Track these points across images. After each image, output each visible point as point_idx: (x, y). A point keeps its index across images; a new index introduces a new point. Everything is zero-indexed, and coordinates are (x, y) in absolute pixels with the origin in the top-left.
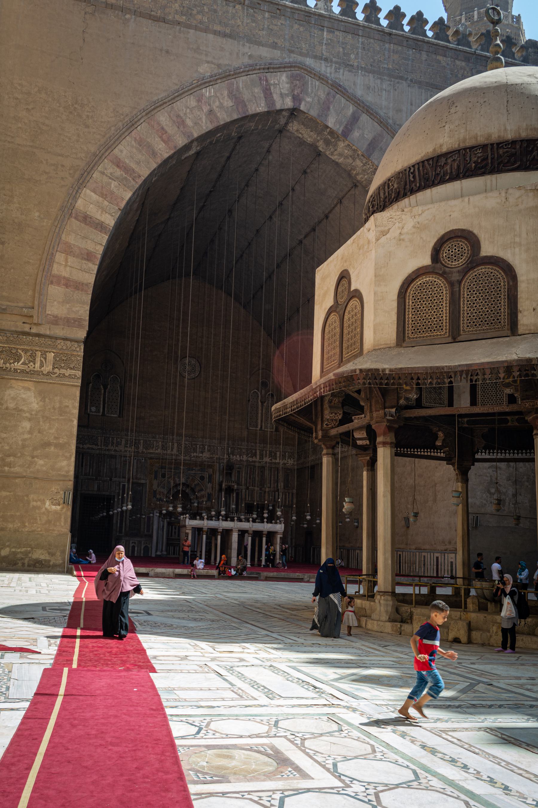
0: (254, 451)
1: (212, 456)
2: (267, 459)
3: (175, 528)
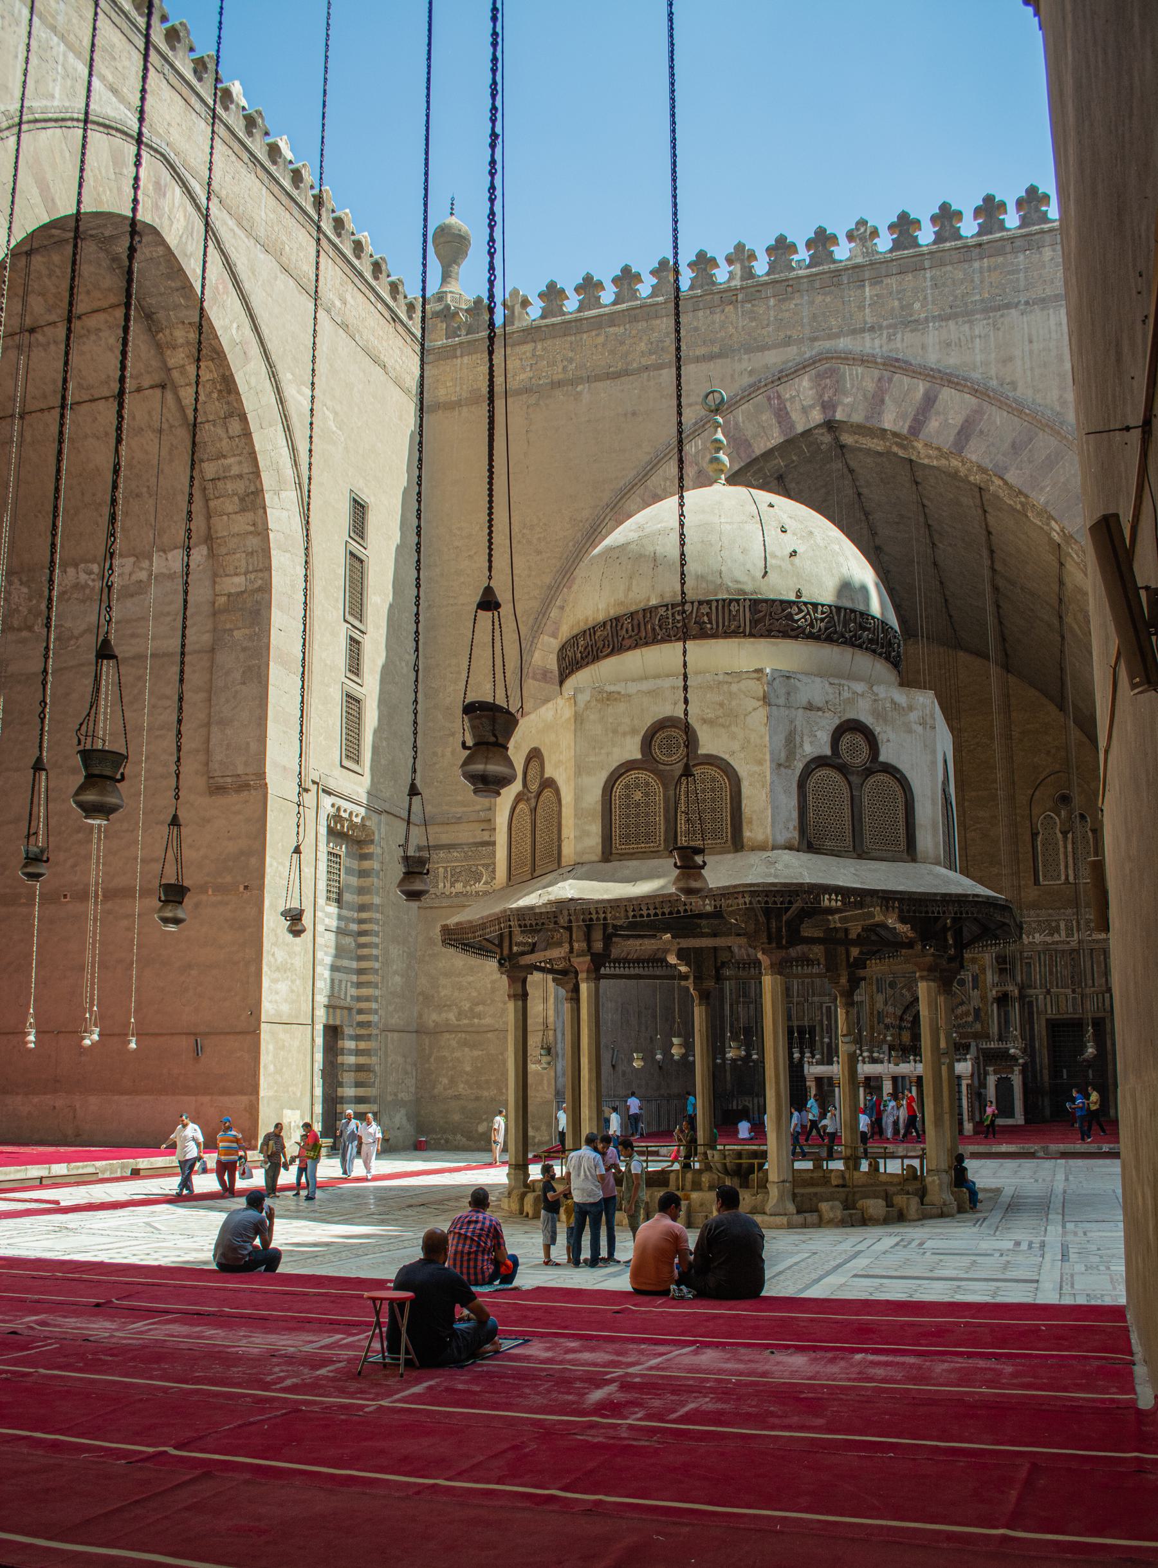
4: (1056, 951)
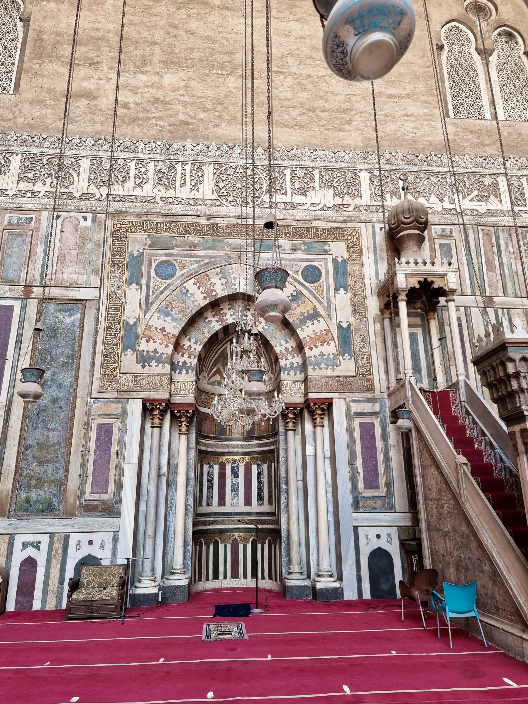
0: (487, 181)
3: (235, 474)
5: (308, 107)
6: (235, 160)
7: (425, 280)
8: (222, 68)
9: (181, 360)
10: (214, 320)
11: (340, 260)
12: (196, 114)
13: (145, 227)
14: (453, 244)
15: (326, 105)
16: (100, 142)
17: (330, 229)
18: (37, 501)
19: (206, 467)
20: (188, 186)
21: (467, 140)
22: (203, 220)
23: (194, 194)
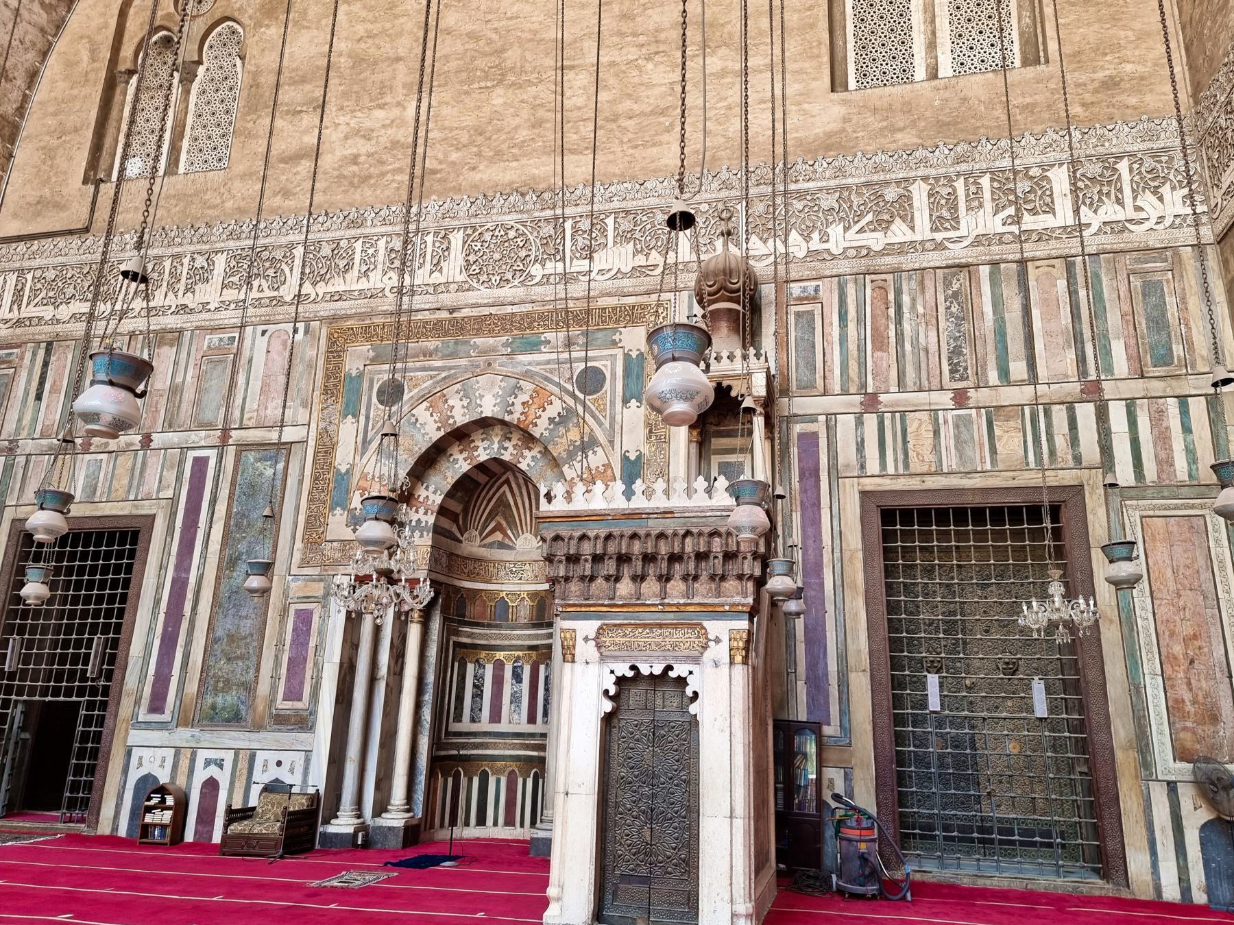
1: (641, 260)
2: (986, 221)
3: (517, 677)
4: (896, 271)
5: (607, 114)
6: (494, 218)
7: (719, 384)
8: (486, 78)
9: (414, 517)
10: (460, 457)
11: (634, 354)
12: (446, 155)
13: (368, 333)
14: (818, 312)
15: (635, 107)
16: (320, 219)
17: (623, 308)
18: (224, 709)
19: (470, 668)
20: (428, 266)
21: (865, 126)
22: (444, 315)
23: (437, 278)
